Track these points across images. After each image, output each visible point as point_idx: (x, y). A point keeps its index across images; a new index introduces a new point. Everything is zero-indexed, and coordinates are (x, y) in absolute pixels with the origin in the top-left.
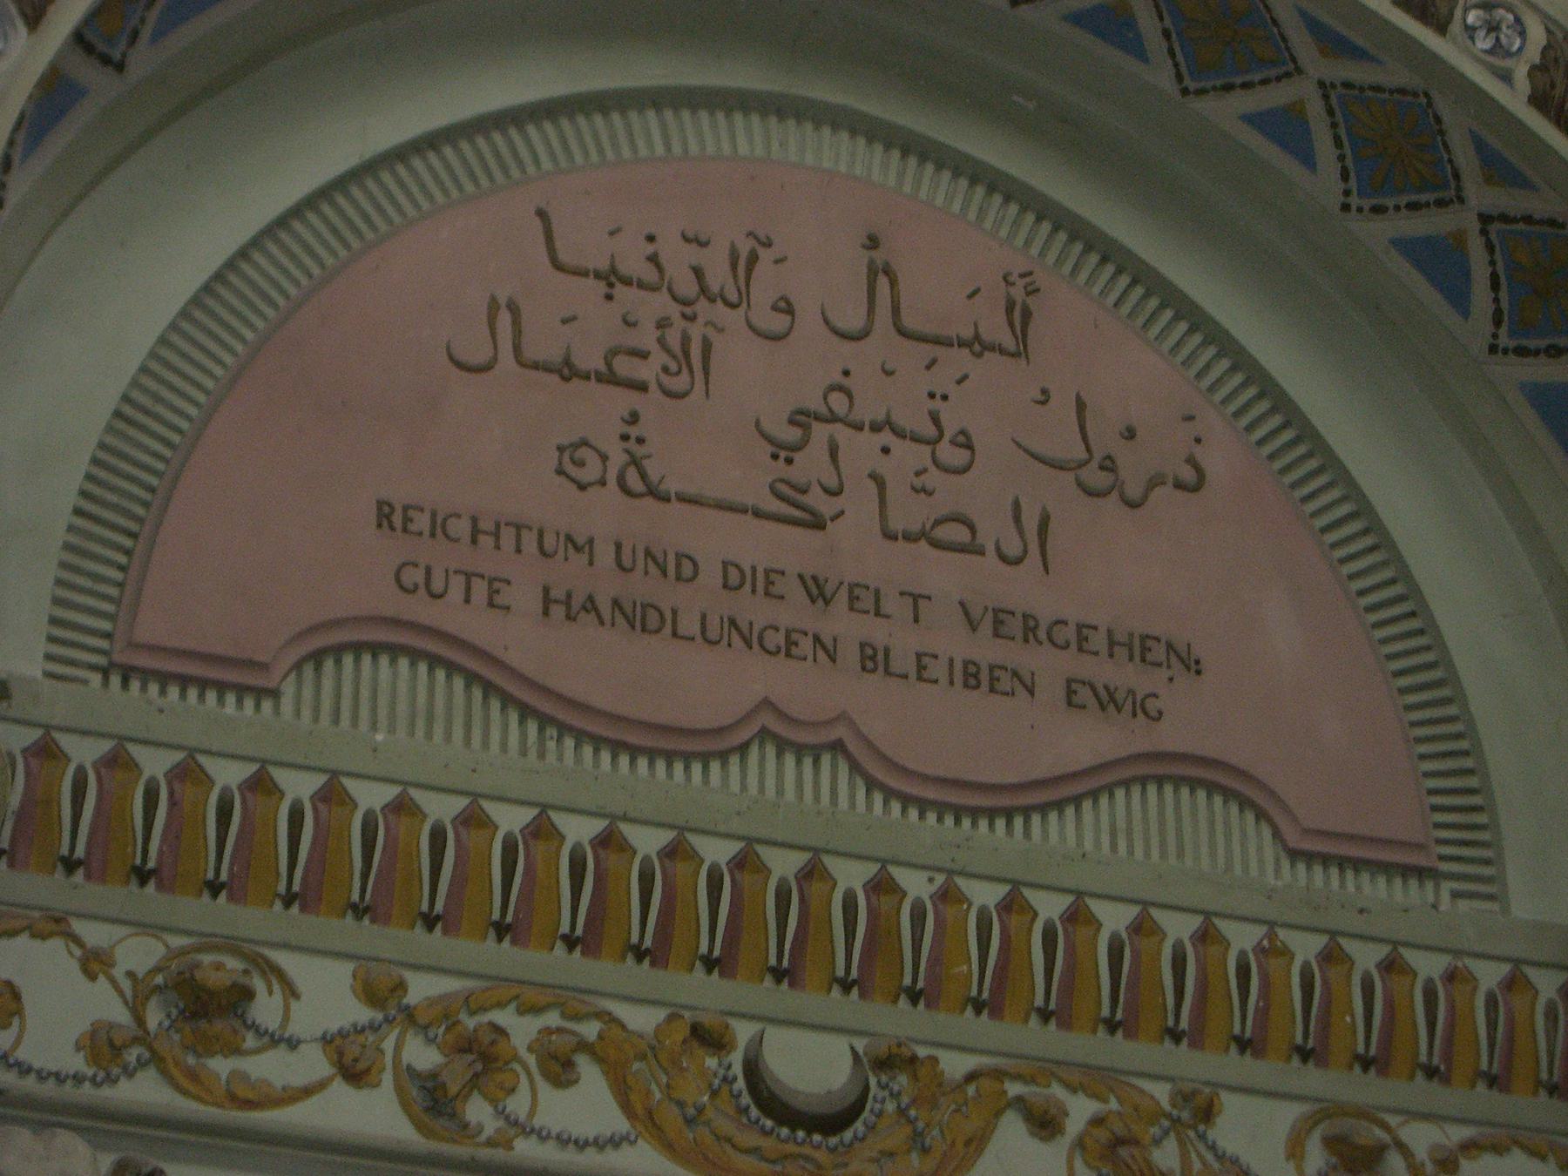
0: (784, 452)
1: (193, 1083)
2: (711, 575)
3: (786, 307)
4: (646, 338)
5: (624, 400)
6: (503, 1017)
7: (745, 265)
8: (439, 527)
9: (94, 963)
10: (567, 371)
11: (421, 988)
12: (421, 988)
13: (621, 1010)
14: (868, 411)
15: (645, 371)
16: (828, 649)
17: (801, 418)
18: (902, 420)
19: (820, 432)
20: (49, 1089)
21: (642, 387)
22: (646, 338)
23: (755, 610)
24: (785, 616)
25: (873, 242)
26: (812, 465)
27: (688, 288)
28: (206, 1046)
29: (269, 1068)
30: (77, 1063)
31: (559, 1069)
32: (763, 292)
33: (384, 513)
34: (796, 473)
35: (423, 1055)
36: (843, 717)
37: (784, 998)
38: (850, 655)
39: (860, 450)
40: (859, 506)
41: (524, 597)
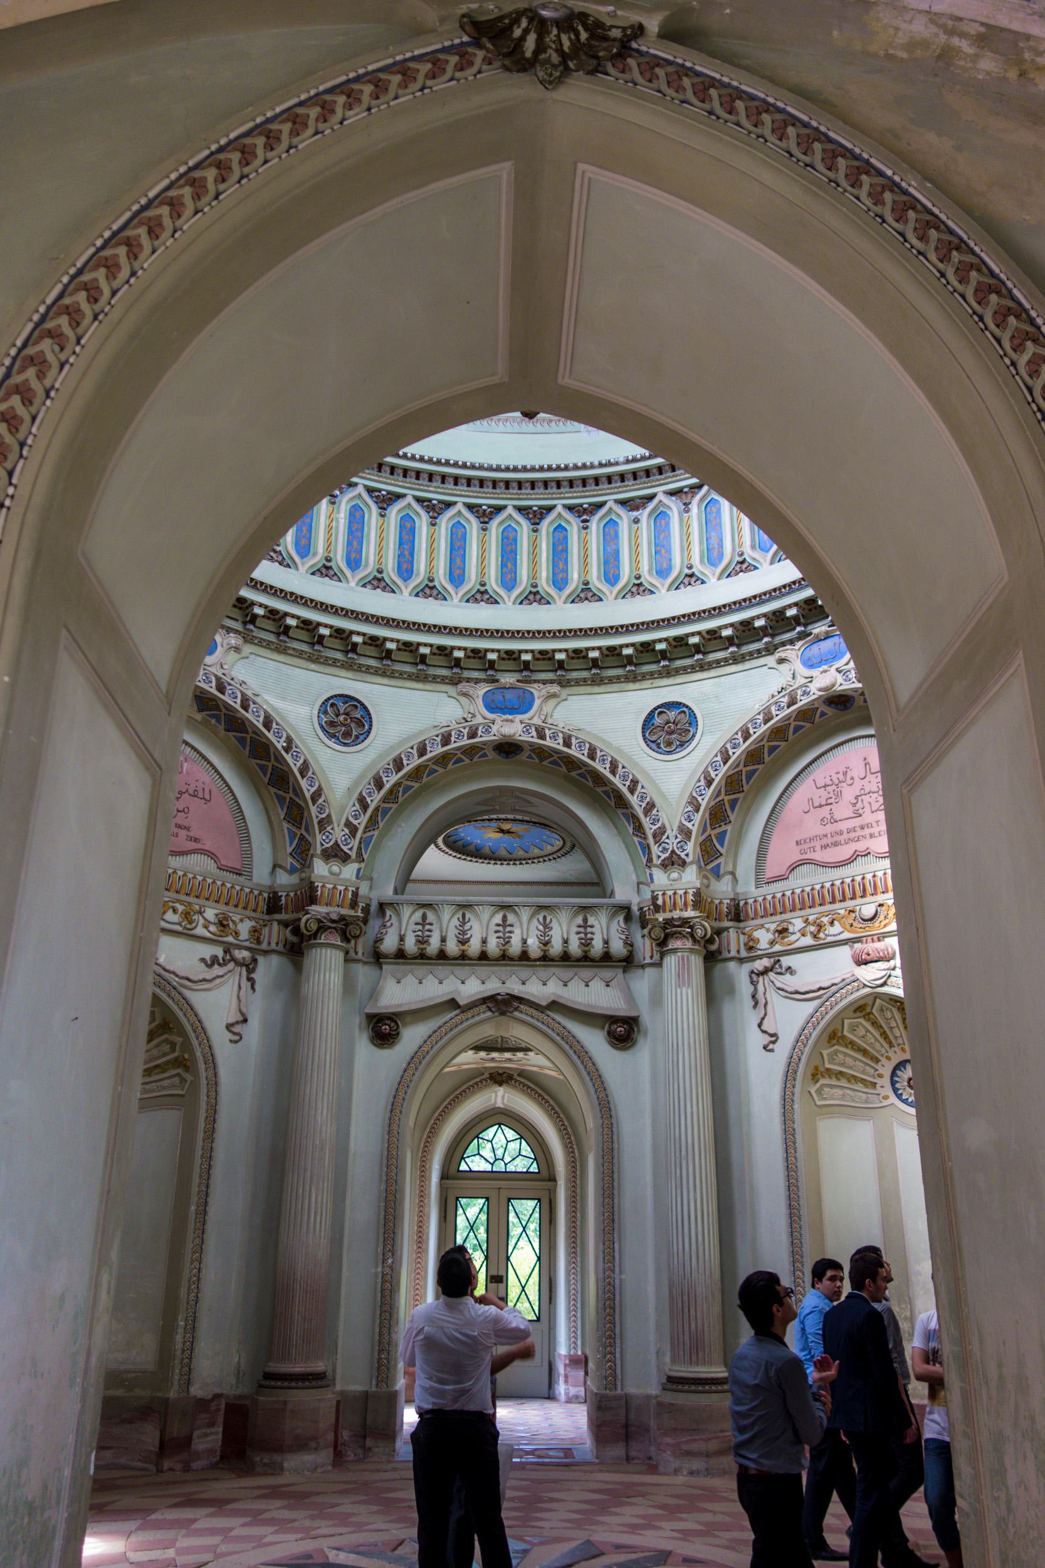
0: (854, 805)
1: (782, 944)
2: (845, 832)
3: (852, 778)
4: (832, 795)
5: (829, 807)
6: (822, 919)
7: (845, 774)
8: (805, 841)
9: (768, 930)
10: (821, 806)
11: (811, 918)
12: (811, 918)
13: (840, 911)
14: (867, 792)
15: (832, 801)
16: (864, 837)
17: (856, 798)
18: (873, 790)
19: (860, 798)
20: (765, 952)
21: (831, 804)
22: (832, 795)
23: (852, 835)
24: (856, 834)
25: (865, 759)
26: (859, 805)
27: (836, 782)
28: (783, 938)
29: (793, 938)
30: (768, 946)
31: (832, 923)
32: (849, 777)
33: (797, 842)
34: (856, 808)
35: (812, 928)
36: (856, 851)
37: (864, 900)
38: (868, 837)
39: (866, 799)
40: (867, 810)
41: (818, 848)
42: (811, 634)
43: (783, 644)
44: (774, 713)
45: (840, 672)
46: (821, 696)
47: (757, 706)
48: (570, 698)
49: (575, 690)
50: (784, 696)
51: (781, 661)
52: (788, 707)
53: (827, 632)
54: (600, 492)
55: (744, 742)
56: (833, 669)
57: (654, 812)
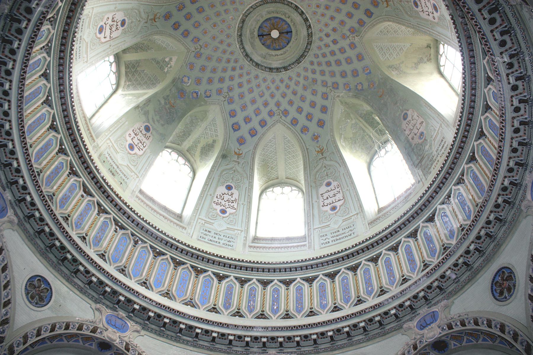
42: (117, 312)
43: (104, 304)
44: (84, 329)
45: (120, 338)
46: (106, 340)
47: (77, 318)
48: (16, 232)
49: (20, 230)
50: (92, 326)
51: (98, 310)
52: (91, 332)
53: (123, 317)
54: (83, 172)
55: (64, 330)
56: (118, 334)
57: (6, 326)
